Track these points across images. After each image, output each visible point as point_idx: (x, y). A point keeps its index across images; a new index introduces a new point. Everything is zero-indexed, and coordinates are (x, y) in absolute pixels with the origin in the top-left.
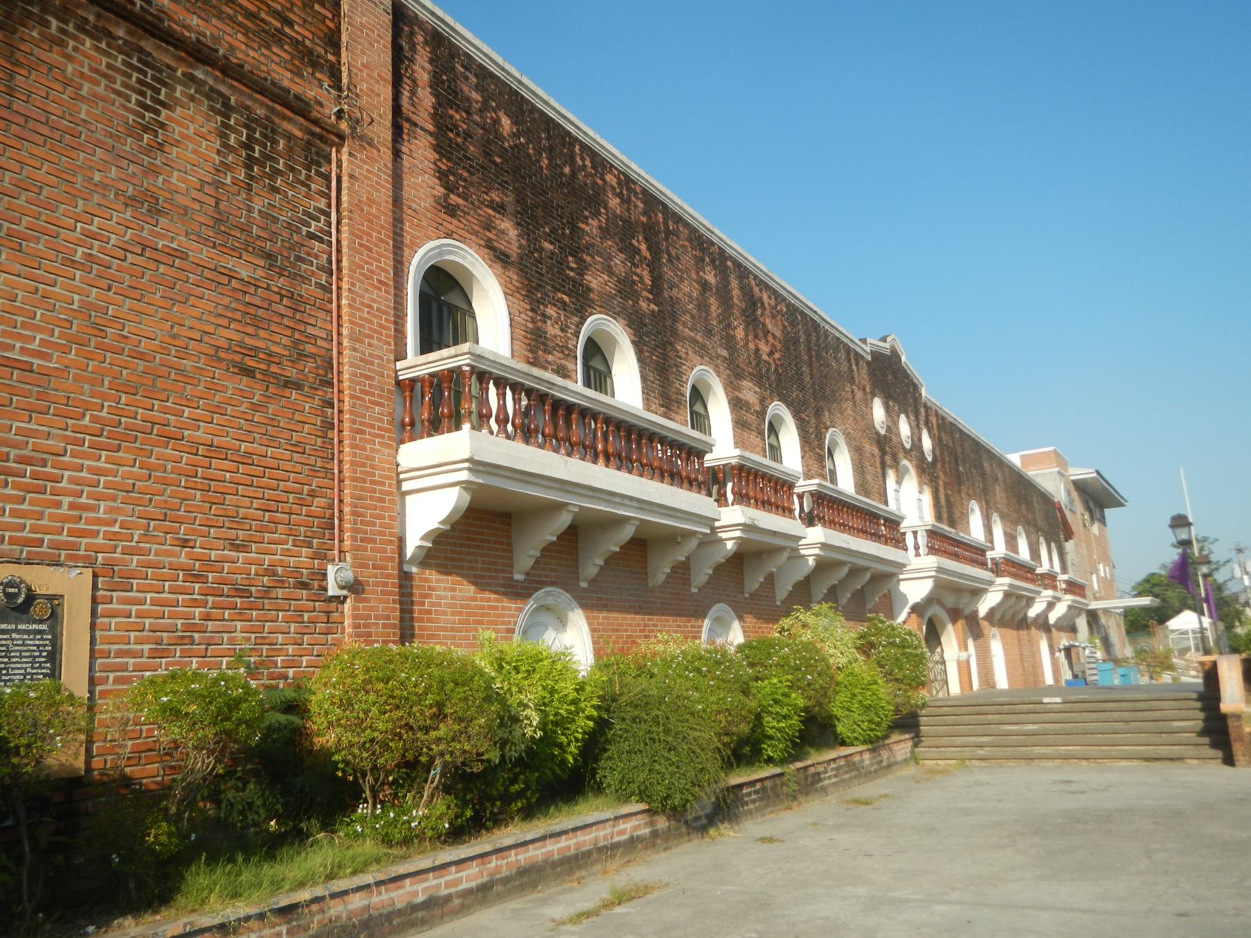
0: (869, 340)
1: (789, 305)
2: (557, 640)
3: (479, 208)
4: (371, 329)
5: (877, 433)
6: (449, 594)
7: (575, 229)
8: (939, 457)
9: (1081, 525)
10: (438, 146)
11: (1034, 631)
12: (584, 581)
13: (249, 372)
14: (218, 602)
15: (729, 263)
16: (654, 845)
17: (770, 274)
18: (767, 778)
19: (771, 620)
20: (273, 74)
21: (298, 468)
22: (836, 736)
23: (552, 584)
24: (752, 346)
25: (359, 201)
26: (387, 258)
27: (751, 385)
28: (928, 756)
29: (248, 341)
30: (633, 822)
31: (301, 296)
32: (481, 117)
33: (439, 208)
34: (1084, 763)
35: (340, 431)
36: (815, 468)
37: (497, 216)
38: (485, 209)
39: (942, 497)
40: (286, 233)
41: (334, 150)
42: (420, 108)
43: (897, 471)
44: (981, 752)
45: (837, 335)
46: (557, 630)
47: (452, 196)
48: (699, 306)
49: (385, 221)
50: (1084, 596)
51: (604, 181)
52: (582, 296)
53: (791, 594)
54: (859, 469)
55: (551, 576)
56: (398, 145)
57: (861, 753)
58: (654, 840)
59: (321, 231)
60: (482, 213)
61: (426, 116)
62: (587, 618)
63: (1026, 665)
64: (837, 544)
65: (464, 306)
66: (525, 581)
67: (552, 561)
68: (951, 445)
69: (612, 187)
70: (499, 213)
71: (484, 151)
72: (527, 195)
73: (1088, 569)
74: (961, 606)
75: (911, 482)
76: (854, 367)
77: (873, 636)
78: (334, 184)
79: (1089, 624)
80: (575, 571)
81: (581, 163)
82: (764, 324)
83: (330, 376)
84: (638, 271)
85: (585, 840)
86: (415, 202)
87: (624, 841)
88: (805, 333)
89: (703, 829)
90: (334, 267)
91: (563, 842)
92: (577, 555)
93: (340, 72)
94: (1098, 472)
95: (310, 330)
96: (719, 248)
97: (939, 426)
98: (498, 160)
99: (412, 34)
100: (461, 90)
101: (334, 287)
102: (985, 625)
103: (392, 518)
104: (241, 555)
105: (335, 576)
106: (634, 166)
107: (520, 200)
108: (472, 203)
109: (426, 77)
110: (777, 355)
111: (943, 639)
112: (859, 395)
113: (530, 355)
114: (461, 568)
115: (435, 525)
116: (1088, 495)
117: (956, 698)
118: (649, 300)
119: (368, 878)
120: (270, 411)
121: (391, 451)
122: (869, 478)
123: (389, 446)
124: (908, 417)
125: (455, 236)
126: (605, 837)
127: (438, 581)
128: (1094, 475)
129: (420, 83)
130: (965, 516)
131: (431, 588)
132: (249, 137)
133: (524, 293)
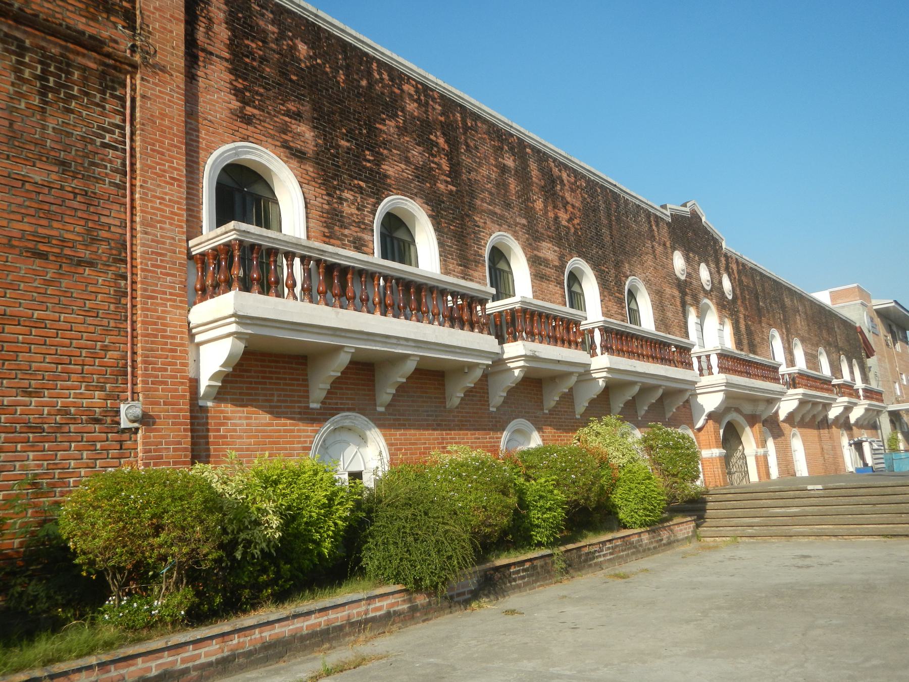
0: (669, 206)
1: (589, 181)
2: (358, 453)
3: (275, 116)
4: (162, 216)
5: (678, 279)
6: (245, 422)
7: (372, 130)
8: (739, 295)
9: (884, 344)
10: (234, 69)
11: (834, 430)
12: (381, 406)
13: (43, 256)
14: (9, 438)
15: (528, 150)
16: (413, 618)
17: (569, 157)
18: (536, 559)
19: (571, 430)
20: (67, 20)
21: (91, 328)
22: (619, 521)
23: (349, 410)
24: (551, 215)
25: (152, 116)
26: (180, 159)
27: (550, 245)
28: (708, 534)
29: (41, 230)
30: (391, 600)
31: (95, 193)
32: (277, 45)
33: (235, 117)
34: (834, 539)
35: (133, 298)
36: (614, 308)
37: (293, 121)
38: (281, 117)
40: (80, 145)
41: (128, 77)
42: (215, 40)
43: (697, 308)
44: (750, 531)
45: (637, 202)
46: (359, 446)
47: (248, 108)
48: (498, 185)
49: (178, 130)
50: (882, 401)
51: (402, 91)
52: (379, 182)
53: (587, 409)
54: (659, 307)
55: (348, 404)
56: (193, 71)
57: (639, 534)
58: (412, 615)
59: (116, 141)
60: (278, 120)
61: (222, 46)
62: (384, 435)
63: (826, 456)
64: (622, 367)
65: (270, 196)
67: (349, 392)
68: (752, 285)
69: (410, 95)
70: (296, 119)
71: (280, 71)
72: (324, 104)
73: (891, 379)
74: (758, 413)
75: (712, 318)
76: (654, 227)
77: (652, 440)
78: (128, 104)
79: (892, 422)
80: (372, 398)
82: (563, 198)
83: (123, 255)
84: (436, 160)
85: (337, 617)
86: (211, 115)
87: (380, 616)
88: (605, 202)
89: (467, 603)
90: (128, 169)
91: (313, 620)
92: (374, 386)
93: (135, 15)
94: (896, 302)
95: (104, 219)
96: (518, 138)
97: (739, 272)
98: (294, 78)
100: (257, 24)
101: (128, 185)
102: (785, 427)
103: (183, 364)
104: (34, 400)
105: (127, 413)
106: (431, 77)
107: (317, 107)
108: (268, 113)
109: (222, 15)
110: (576, 221)
112: (659, 249)
113: (326, 230)
114: (258, 400)
115: (217, 368)
116: (891, 320)
117: (755, 485)
118: (447, 182)
119: (93, 660)
120: (63, 285)
121: (182, 312)
122: (670, 314)
123: (182, 308)
124: (708, 265)
125: (251, 139)
126: (358, 614)
127: (232, 412)
128: (893, 304)
129: (215, 21)
130: (767, 341)
131: (225, 418)
132: (43, 71)
133: (319, 181)
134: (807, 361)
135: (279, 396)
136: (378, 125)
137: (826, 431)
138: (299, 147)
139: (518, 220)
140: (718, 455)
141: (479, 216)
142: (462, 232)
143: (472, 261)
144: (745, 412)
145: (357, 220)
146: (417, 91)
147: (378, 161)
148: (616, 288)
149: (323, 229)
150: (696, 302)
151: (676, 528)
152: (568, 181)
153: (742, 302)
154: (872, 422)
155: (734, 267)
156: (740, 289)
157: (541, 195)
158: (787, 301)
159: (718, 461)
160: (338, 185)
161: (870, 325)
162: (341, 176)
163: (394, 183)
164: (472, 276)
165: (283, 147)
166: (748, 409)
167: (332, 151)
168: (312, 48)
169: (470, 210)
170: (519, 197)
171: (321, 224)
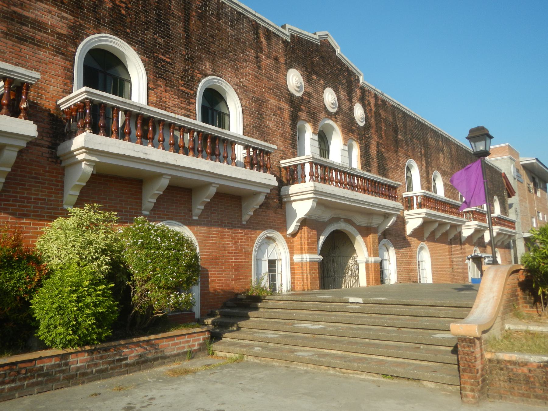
0: (288, 26)
9: (526, 189)
11: (467, 246)
39: (373, 151)
43: (315, 125)
45: (240, 10)
50: (514, 228)
57: (64, 357)
63: (455, 267)
68: (391, 119)
73: (529, 215)
76: (263, 40)
94: (537, 159)
97: (376, 105)
111: (356, 246)
112: (266, 62)
116: (534, 174)
117: (363, 288)
124: (336, 91)
128: (535, 161)
134: (446, 191)
137: (459, 246)
140: (308, 260)
144: (358, 224)
148: (181, 82)
150: (314, 119)
151: (165, 342)
153: (377, 131)
154: (506, 243)
155: (372, 101)
156: (376, 120)
158: (431, 141)
159: (308, 266)
161: (516, 174)
166: (361, 221)
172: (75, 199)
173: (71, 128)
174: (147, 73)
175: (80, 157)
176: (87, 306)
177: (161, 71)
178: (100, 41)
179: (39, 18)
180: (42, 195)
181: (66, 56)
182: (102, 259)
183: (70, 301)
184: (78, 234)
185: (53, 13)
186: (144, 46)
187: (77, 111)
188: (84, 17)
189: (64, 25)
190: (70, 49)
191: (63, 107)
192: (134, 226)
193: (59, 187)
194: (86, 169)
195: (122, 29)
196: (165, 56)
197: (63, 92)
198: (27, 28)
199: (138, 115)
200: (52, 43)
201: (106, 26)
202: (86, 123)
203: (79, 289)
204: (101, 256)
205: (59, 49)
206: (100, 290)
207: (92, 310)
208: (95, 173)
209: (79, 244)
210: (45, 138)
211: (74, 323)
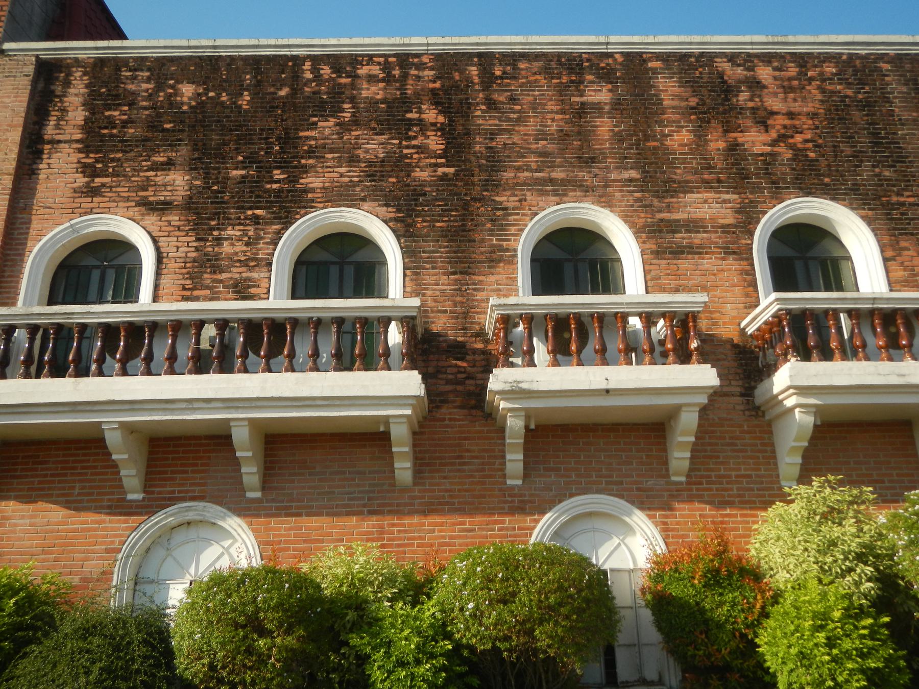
3: (133, 176)
7: (289, 141)
23: (193, 499)
47: (97, 180)
55: (194, 491)
56: (35, 166)
66: (144, 499)
67: (198, 475)
81: (311, 76)
84: (414, 142)
99: (69, 74)
108: (124, 176)
109: (78, 100)
110: (799, 138)
113: (189, 282)
114: (52, 495)
125: (94, 211)
133: (187, 228)
135: (83, 488)
136: (301, 134)
138: (162, 198)
139: (613, 176)
141: (508, 193)
142: (463, 225)
143: (484, 262)
145: (243, 259)
146: (386, 67)
147: (294, 177)
149: (183, 282)
152: (775, 78)
157: (691, 121)
160: (218, 224)
162: (224, 213)
163: (320, 195)
164: (480, 283)
165: (138, 204)
167: (216, 188)
168: (204, 83)
169: (487, 190)
170: (621, 141)
171: (181, 276)
172: (796, 471)
173: (768, 359)
174: (876, 235)
175: (789, 403)
176: (847, 655)
177: (902, 224)
178: (785, 213)
179: (693, 215)
180: (746, 470)
181: (740, 254)
182: (858, 571)
183: (816, 645)
184: (810, 530)
185: (710, 201)
186: (860, 194)
187: (770, 331)
188: (754, 188)
189: (728, 211)
190: (744, 241)
191: (750, 330)
192: (906, 510)
193: (769, 454)
194: (803, 420)
195: (816, 181)
196: (902, 195)
197: (746, 307)
198: (680, 235)
199: (872, 312)
200: (717, 243)
201: (789, 188)
202: (788, 347)
203: (828, 625)
204: (857, 565)
205: (728, 248)
206: (864, 628)
207: (857, 663)
208: (819, 423)
209: (815, 546)
210: (733, 383)
211: (831, 684)
